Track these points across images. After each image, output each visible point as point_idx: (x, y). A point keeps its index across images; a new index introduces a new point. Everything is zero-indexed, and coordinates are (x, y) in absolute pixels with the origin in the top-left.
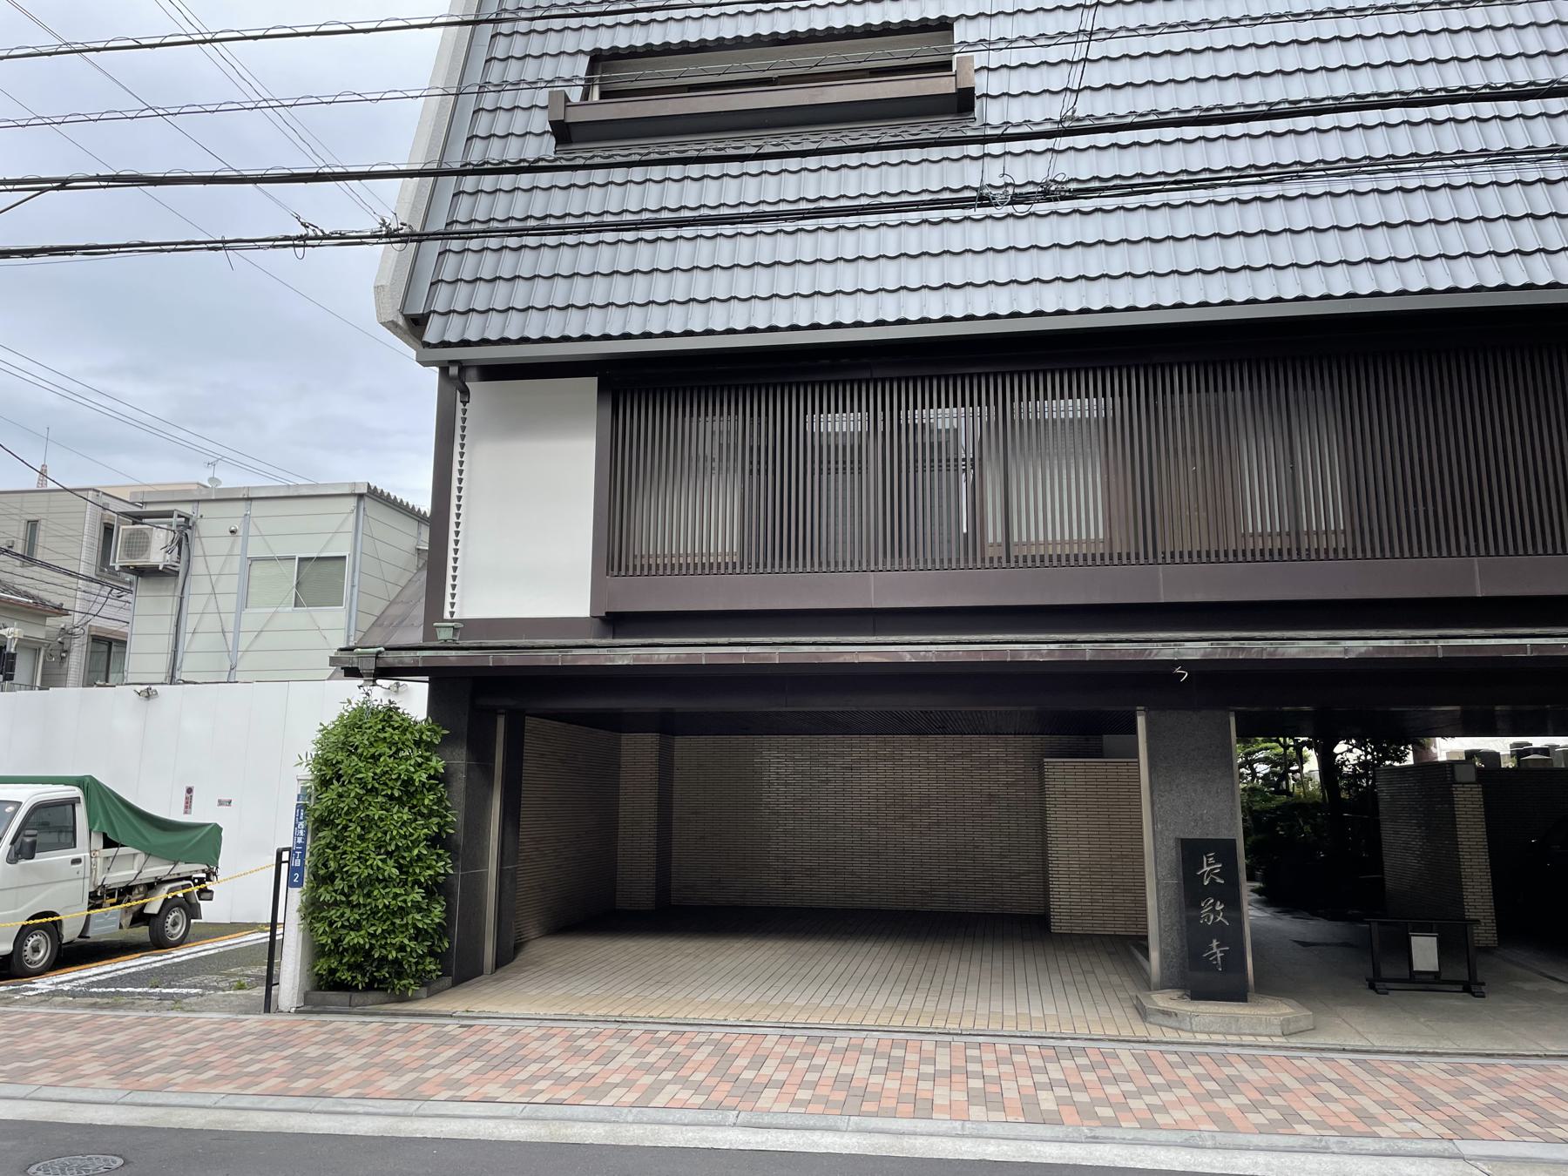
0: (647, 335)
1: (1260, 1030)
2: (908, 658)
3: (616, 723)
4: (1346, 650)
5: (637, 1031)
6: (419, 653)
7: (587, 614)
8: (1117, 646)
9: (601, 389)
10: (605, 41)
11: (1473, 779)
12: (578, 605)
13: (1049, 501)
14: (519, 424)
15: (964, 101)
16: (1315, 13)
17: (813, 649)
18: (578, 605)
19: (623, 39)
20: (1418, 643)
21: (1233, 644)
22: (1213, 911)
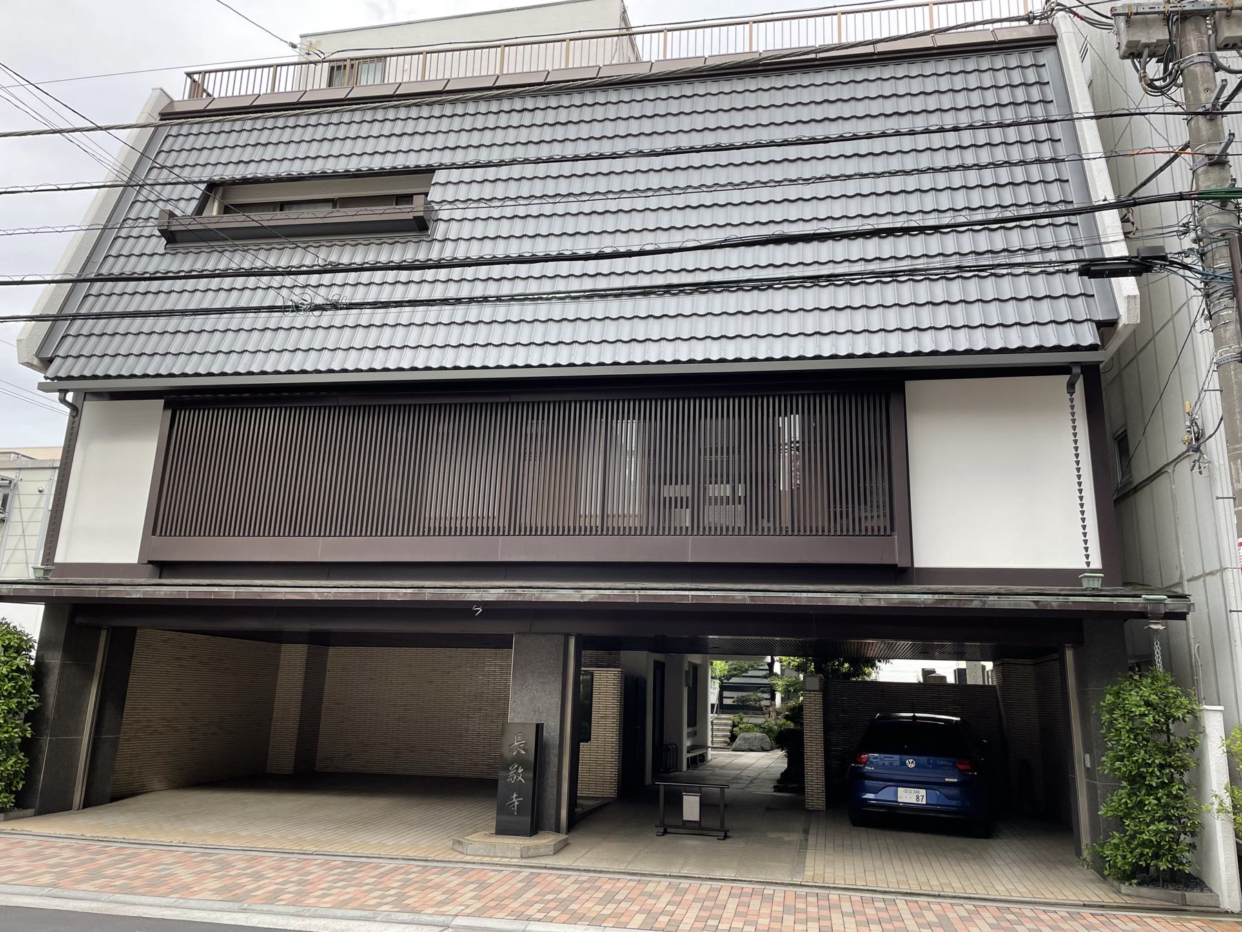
0: (304, 372)
1: (508, 854)
2: (316, 597)
3: (278, 638)
4: (582, 597)
5: (338, 862)
6: (14, 586)
7: (134, 559)
8: (448, 591)
9: (165, 407)
10: (218, 174)
11: (817, 688)
12: (129, 554)
13: (611, 494)
14: (118, 430)
15: (420, 226)
16: (791, 181)
17: (259, 590)
18: (129, 554)
19: (230, 173)
20: (629, 592)
21: (519, 591)
22: (516, 773)
